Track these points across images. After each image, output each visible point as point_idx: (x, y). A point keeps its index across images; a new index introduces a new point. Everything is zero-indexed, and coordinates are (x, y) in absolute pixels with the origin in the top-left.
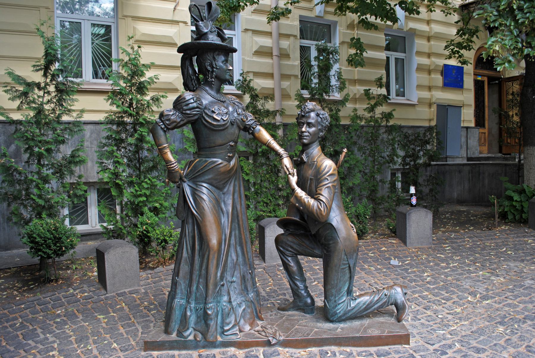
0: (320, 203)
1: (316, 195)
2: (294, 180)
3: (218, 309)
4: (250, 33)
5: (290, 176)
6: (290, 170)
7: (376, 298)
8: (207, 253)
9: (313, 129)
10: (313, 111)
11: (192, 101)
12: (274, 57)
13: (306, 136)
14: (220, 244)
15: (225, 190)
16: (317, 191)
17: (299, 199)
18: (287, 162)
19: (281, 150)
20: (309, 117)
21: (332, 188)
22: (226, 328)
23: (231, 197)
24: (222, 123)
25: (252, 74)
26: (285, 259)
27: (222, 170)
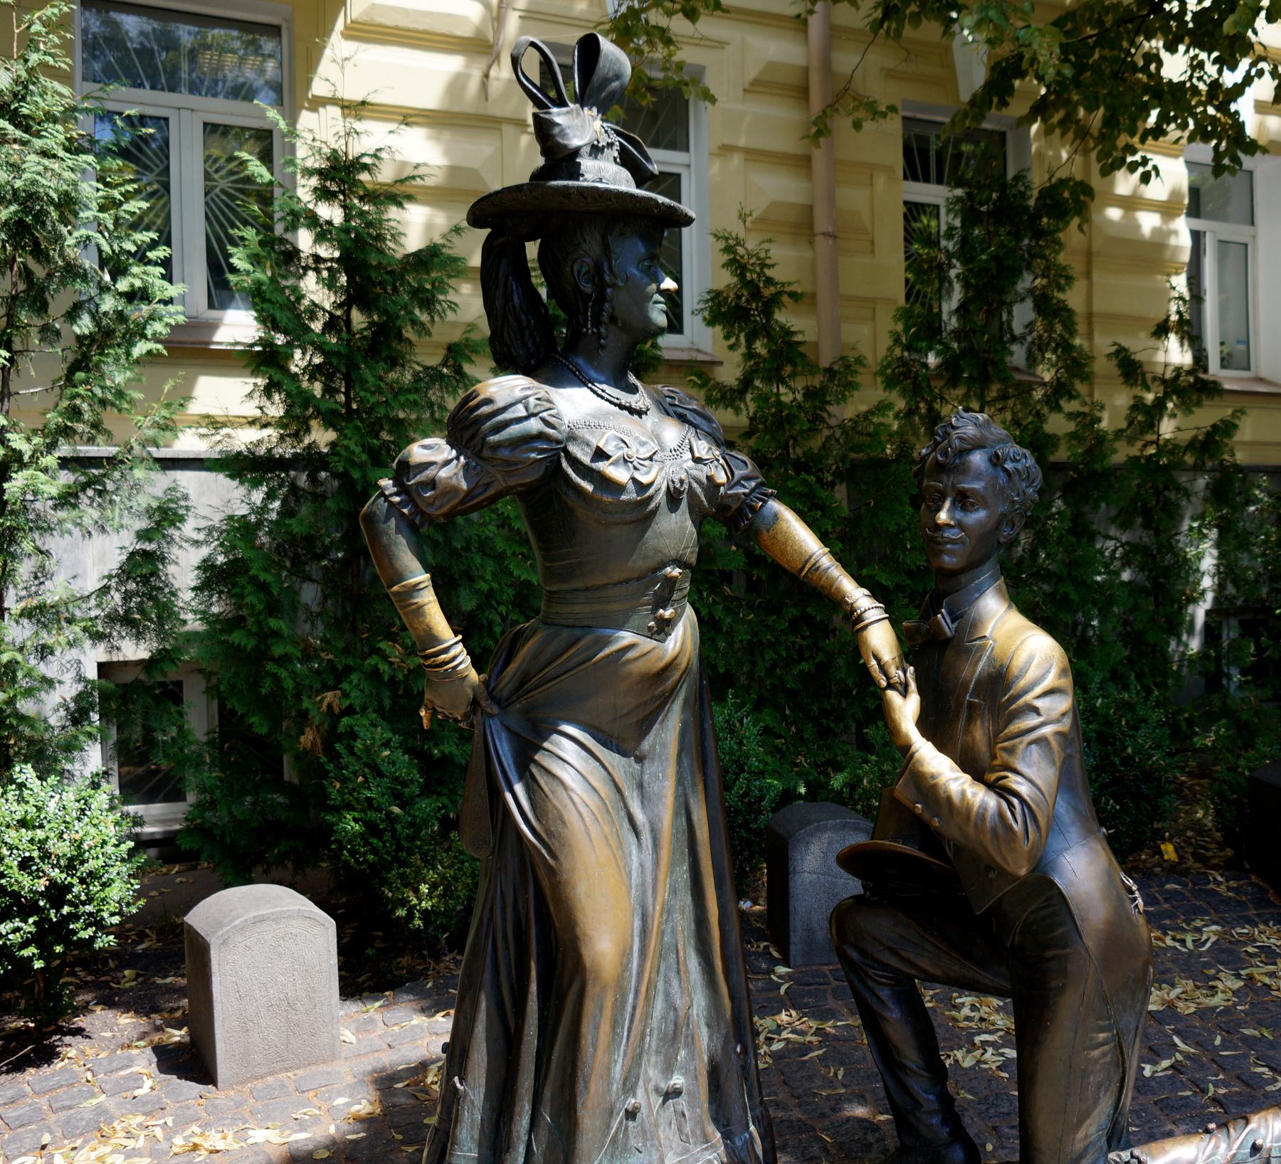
0: (1011, 805)
1: (993, 770)
2: (906, 709)
4: (736, 160)
5: (893, 695)
6: (893, 671)
8: (576, 986)
9: (981, 515)
10: (978, 445)
11: (520, 411)
12: (819, 240)
13: (954, 542)
16: (994, 757)
17: (926, 788)
18: (881, 639)
19: (859, 597)
20: (963, 469)
21: (1054, 744)
24: (630, 495)
26: (867, 996)
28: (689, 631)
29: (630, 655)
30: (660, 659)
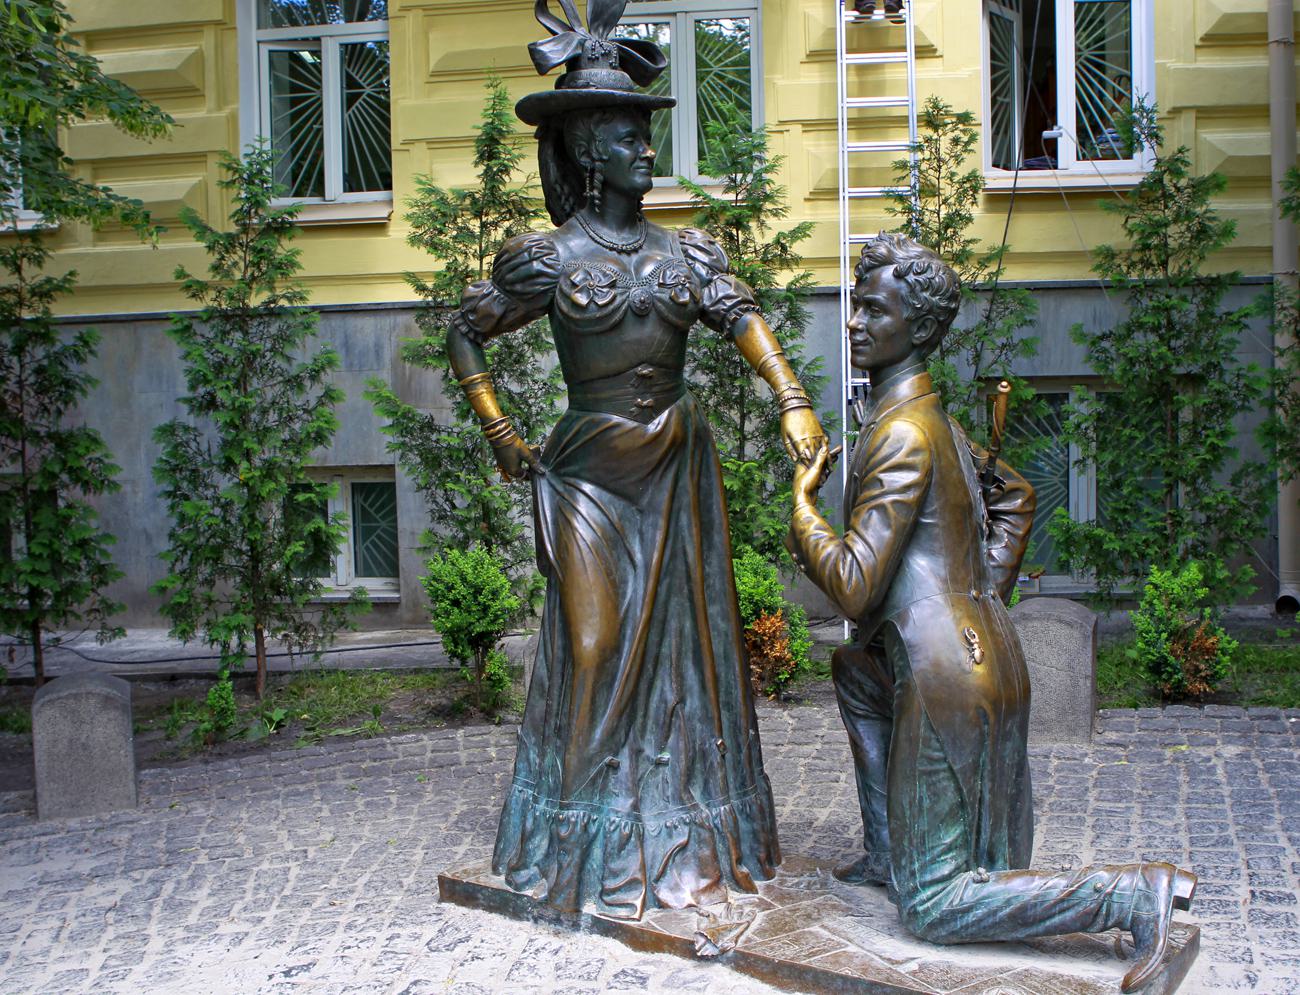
3: (593, 829)
6: (802, 448)
7: (1055, 894)
9: (886, 320)
14: (610, 650)
15: (645, 501)
22: (611, 884)
23: (662, 523)
25: (1192, 115)
27: (622, 444)
28: (673, 418)
29: (616, 432)
30: (643, 436)
